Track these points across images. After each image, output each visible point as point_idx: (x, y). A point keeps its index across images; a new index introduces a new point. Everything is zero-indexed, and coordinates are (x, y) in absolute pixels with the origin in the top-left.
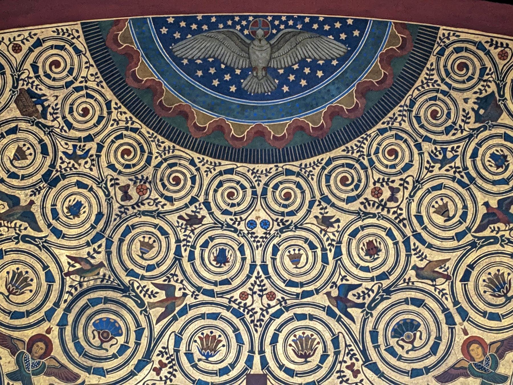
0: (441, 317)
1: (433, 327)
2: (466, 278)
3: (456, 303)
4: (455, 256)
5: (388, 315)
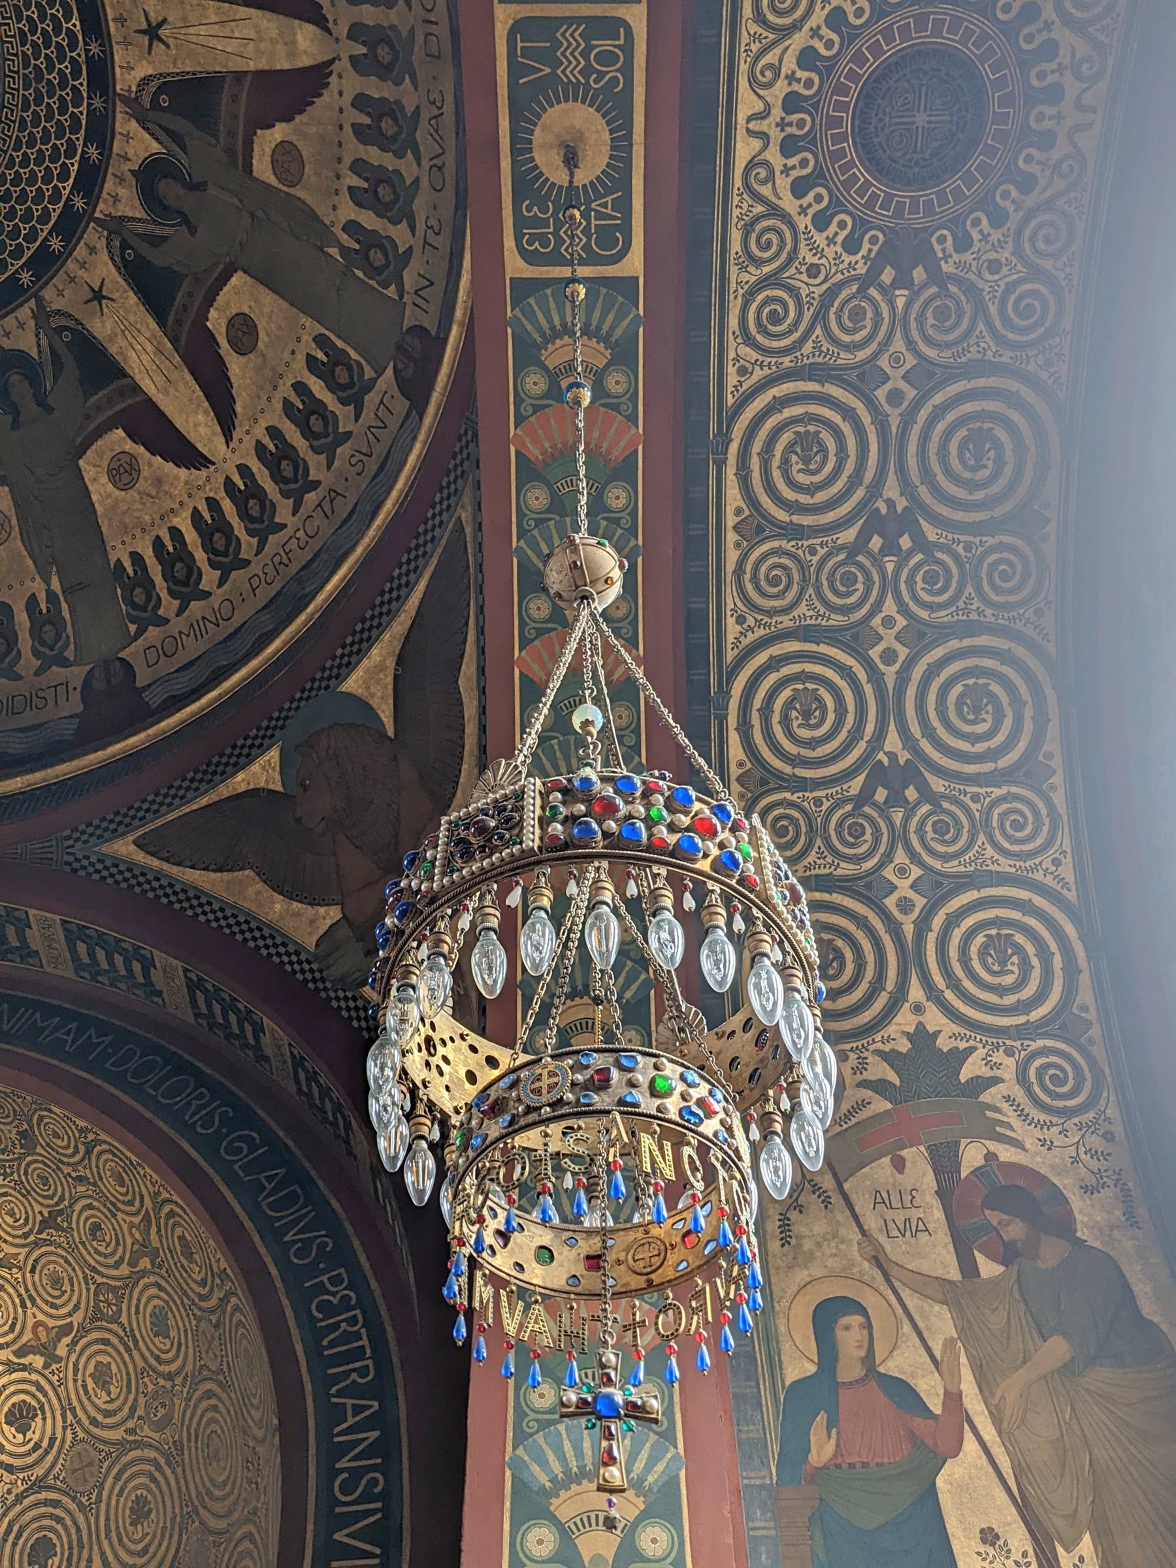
0: (17, 1301)
1: (11, 1309)
2: (33, 1271)
3: (27, 1290)
4: (24, 1251)
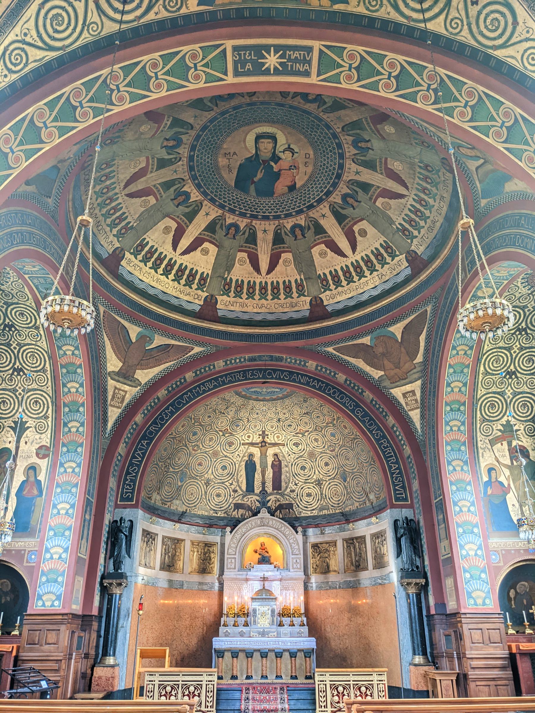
5: (287, 423)
